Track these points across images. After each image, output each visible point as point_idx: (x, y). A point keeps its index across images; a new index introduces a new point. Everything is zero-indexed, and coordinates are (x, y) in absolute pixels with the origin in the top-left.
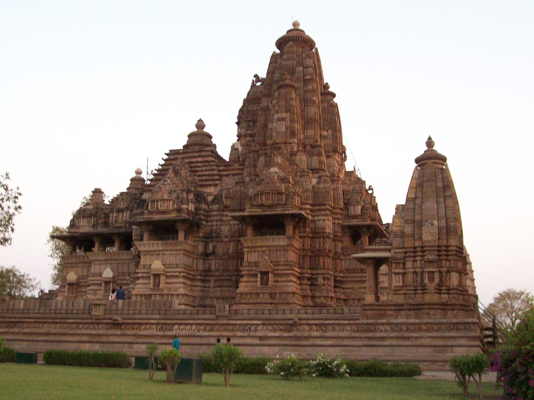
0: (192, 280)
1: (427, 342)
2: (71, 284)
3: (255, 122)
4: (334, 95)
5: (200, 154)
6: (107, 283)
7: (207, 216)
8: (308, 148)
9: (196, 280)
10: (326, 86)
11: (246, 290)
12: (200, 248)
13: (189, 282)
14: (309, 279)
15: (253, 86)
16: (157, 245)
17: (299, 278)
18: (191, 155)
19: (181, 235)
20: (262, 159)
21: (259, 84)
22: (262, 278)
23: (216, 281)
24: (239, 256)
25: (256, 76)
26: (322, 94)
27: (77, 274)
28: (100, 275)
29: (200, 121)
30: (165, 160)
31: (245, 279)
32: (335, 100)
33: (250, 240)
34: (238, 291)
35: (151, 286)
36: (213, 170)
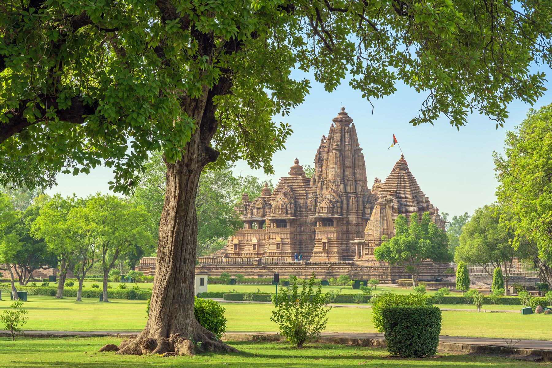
0: (294, 245)
1: (374, 273)
2: (236, 245)
3: (322, 164)
4: (362, 149)
5: (297, 181)
6: (254, 245)
7: (300, 214)
8: (346, 181)
9: (297, 244)
10: (358, 145)
11: (317, 250)
12: (298, 229)
13: (293, 246)
14: (346, 244)
15: (322, 143)
16: (278, 230)
17: (341, 244)
18: (292, 181)
19: (288, 225)
20: (324, 186)
21: (325, 141)
22: (323, 245)
23: (305, 244)
24: (314, 232)
25: (324, 136)
26: (355, 150)
27: (238, 239)
28: (250, 240)
29: (297, 159)
30: (280, 183)
31: (317, 245)
32: (362, 152)
33: (319, 227)
34: (315, 250)
35: (276, 248)
36: (302, 190)
